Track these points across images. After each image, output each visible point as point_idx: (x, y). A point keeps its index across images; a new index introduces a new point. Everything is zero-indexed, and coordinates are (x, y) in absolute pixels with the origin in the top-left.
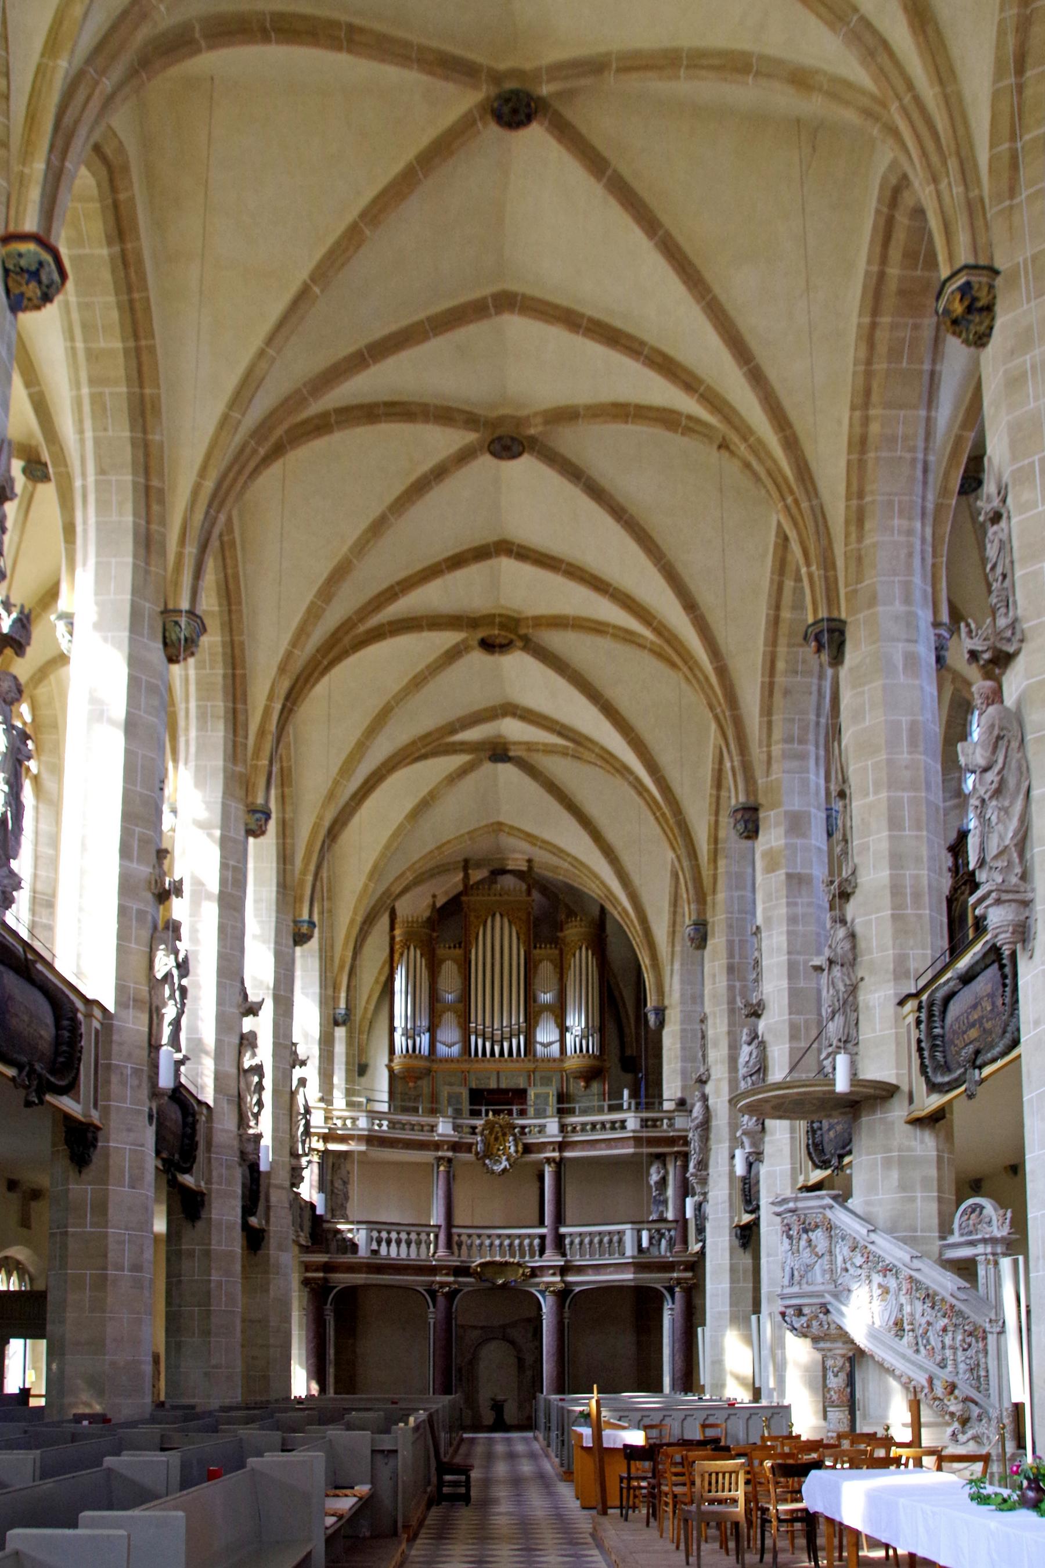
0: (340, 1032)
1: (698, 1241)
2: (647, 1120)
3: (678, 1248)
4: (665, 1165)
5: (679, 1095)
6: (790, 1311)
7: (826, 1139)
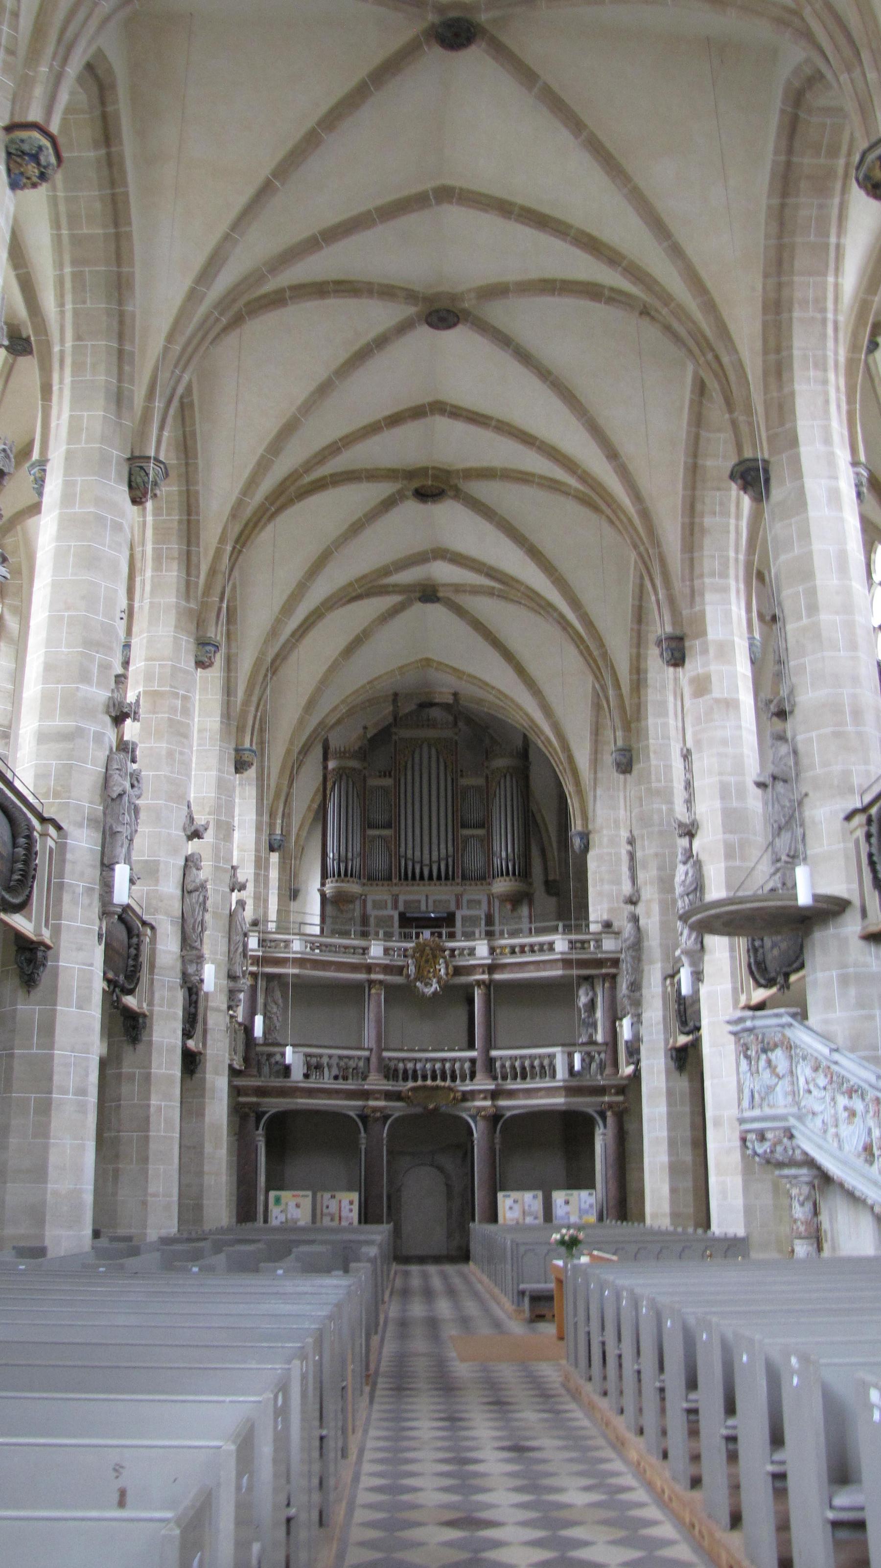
0: (275, 857)
1: (628, 1064)
2: (576, 942)
3: (608, 1071)
4: (593, 988)
5: (605, 917)
6: (752, 1137)
7: (769, 957)
